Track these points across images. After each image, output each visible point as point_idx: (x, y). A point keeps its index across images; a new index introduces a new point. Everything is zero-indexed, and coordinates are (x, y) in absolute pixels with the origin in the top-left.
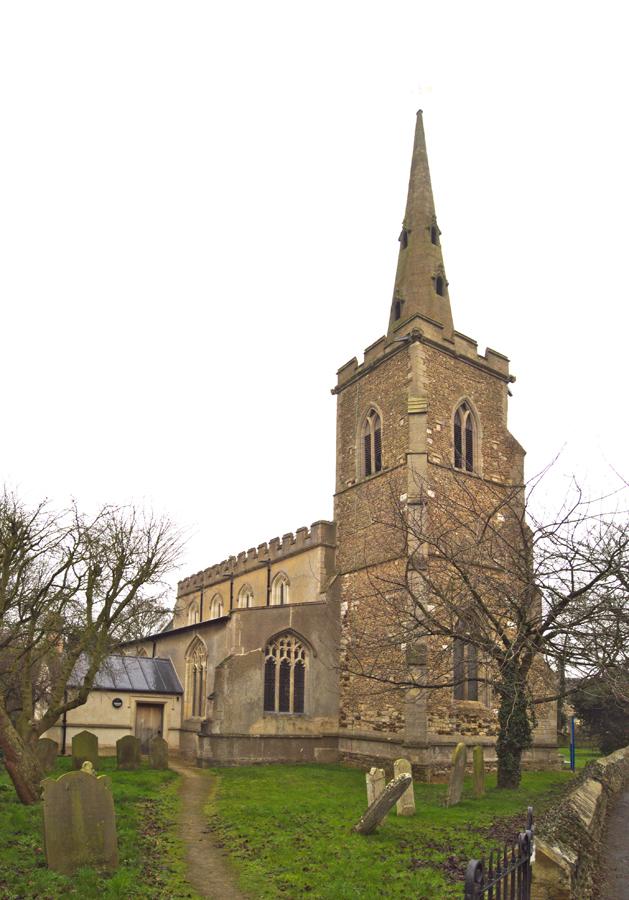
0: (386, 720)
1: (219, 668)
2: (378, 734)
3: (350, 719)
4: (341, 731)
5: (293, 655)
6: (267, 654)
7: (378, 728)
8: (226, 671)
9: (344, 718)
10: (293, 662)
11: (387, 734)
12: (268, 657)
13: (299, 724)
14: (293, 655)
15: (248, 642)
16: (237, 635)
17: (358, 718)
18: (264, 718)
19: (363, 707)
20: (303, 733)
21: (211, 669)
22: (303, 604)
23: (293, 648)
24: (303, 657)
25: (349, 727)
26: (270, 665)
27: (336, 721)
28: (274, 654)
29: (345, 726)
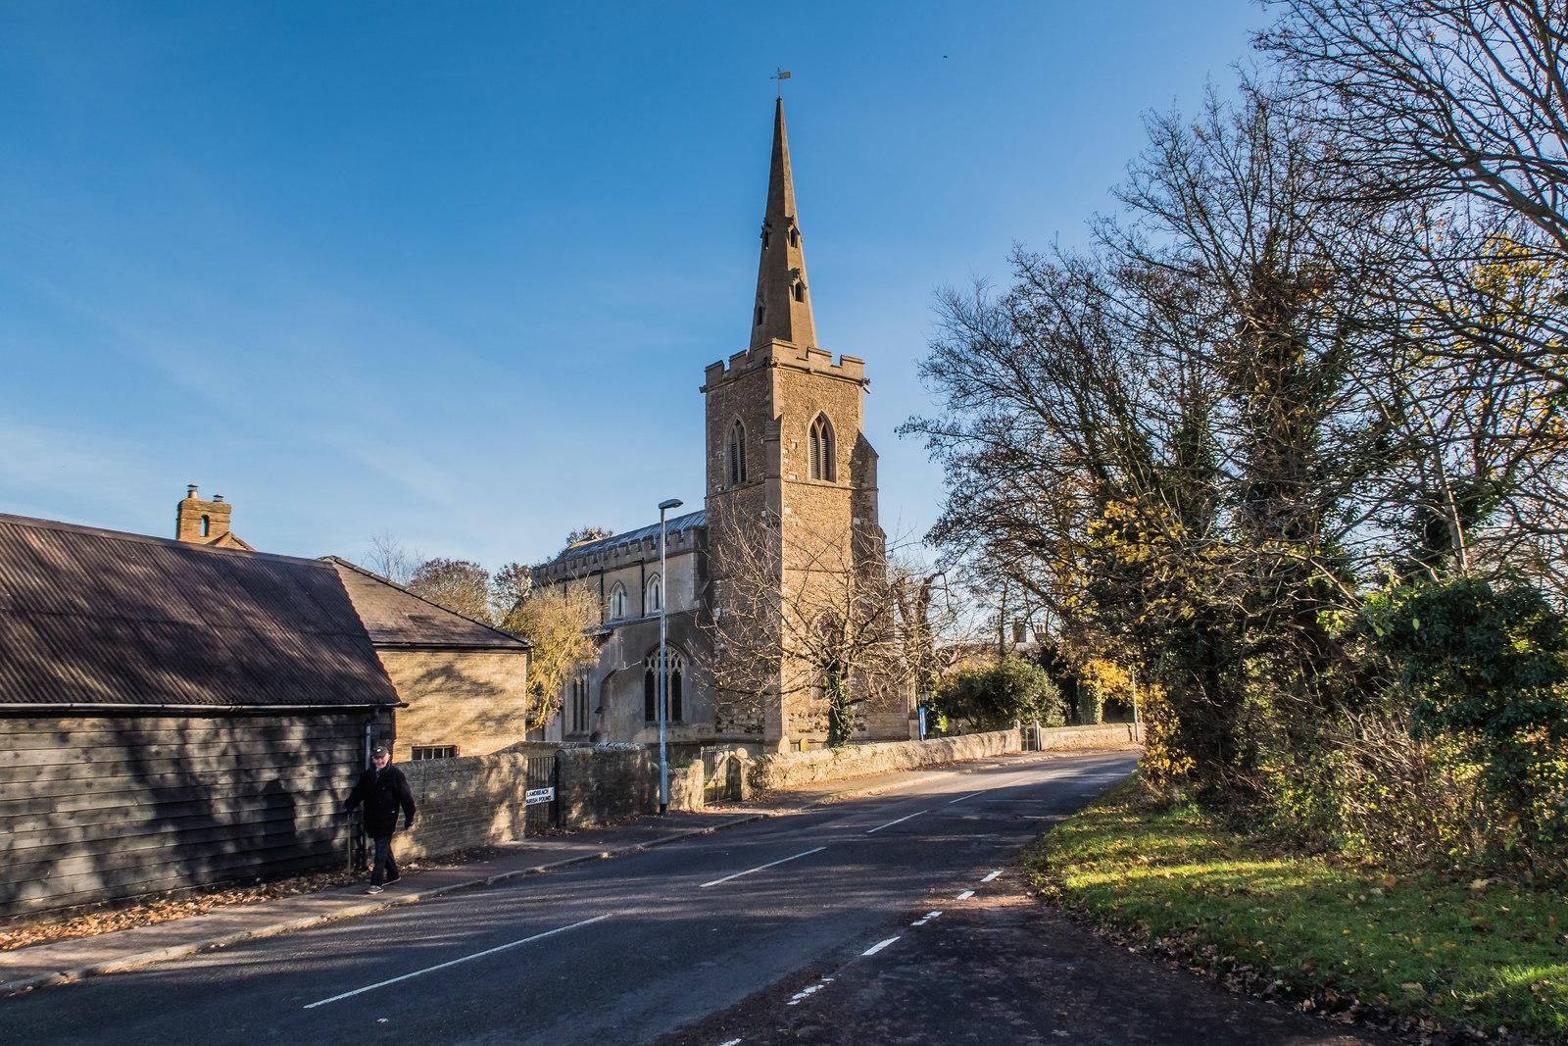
0: (754, 722)
1: (605, 681)
2: (748, 736)
3: (725, 723)
4: (718, 735)
5: (670, 664)
6: (647, 665)
7: (748, 730)
8: (611, 685)
9: (719, 723)
10: (670, 672)
11: (756, 736)
12: (647, 669)
13: (678, 731)
14: (670, 664)
15: (630, 656)
16: (619, 650)
17: (732, 722)
18: (646, 728)
19: (735, 711)
20: (682, 740)
21: (594, 682)
22: (678, 614)
23: (670, 657)
24: (680, 665)
25: (725, 731)
26: (650, 676)
27: (711, 726)
28: (653, 665)
29: (720, 730)
